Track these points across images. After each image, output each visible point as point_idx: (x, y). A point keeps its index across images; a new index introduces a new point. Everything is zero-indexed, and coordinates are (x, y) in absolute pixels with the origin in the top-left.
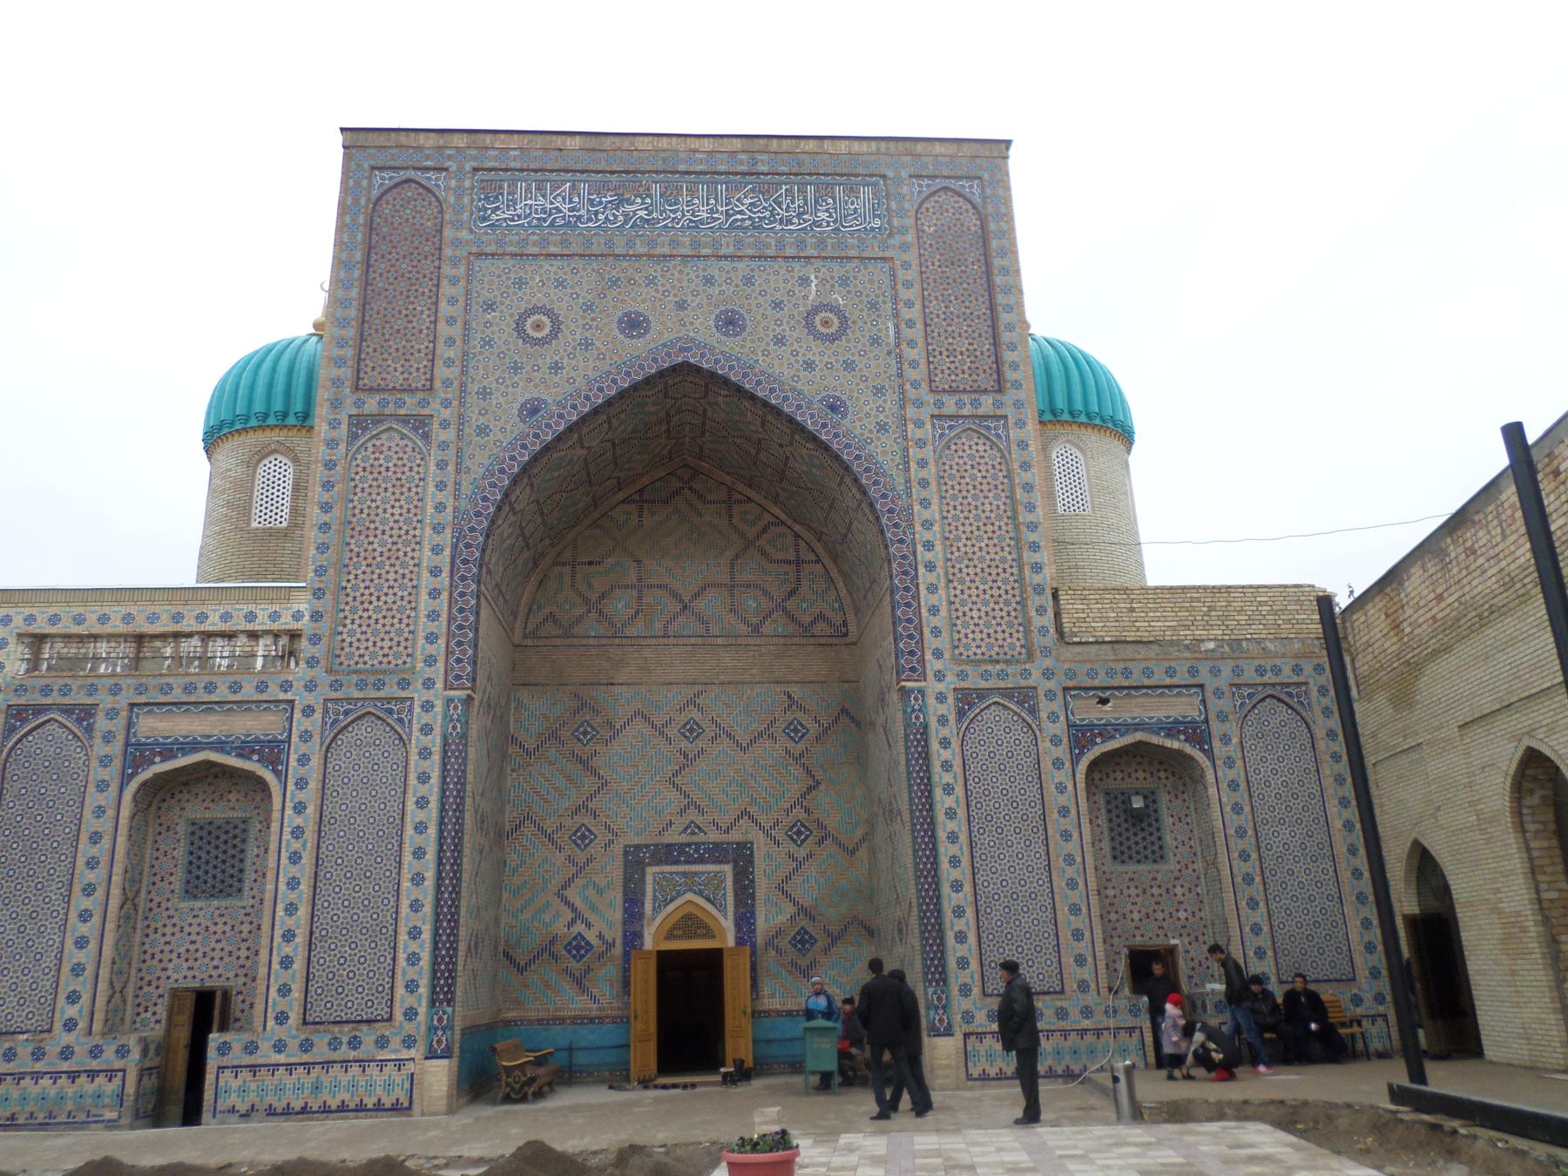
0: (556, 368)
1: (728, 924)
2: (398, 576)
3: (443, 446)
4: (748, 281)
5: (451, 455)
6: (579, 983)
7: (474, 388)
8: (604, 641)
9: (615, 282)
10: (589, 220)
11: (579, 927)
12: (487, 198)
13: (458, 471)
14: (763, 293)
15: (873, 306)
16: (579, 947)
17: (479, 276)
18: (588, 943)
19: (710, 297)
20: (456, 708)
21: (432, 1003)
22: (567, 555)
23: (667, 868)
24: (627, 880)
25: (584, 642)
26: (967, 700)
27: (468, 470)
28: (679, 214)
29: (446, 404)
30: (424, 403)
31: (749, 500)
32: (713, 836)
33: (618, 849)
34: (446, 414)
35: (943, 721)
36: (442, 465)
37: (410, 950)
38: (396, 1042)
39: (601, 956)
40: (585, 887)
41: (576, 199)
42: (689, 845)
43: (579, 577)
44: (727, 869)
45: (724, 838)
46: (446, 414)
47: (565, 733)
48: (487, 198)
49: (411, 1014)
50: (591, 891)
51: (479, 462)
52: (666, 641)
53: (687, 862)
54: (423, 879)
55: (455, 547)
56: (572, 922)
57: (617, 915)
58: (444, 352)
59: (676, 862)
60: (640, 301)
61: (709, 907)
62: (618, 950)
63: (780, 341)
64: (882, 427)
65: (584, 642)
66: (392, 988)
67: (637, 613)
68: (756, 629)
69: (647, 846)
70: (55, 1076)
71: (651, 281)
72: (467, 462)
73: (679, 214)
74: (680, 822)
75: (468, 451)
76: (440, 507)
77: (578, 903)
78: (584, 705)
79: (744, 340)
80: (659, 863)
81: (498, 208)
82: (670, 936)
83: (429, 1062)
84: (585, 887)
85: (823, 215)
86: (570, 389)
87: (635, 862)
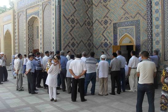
11: (106, 41)
16: (106, 45)
18: (108, 44)
24: (114, 30)
32: (131, 19)
33: (112, 24)
39: (110, 46)
44: (134, 27)
50: (108, 34)
56: (105, 40)
57: (113, 38)
59: (123, 26)
69: (118, 23)
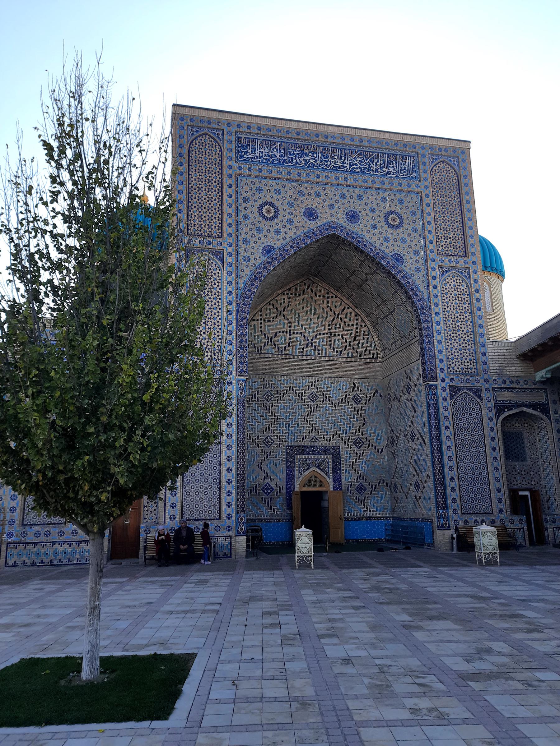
0: (277, 232)
1: (330, 481)
2: (213, 324)
3: (230, 265)
4: (360, 197)
5: (233, 269)
6: (268, 504)
7: (241, 238)
8: (275, 356)
9: (302, 194)
10: (289, 162)
11: (268, 481)
12: (242, 146)
13: (237, 277)
14: (366, 204)
15: (413, 214)
16: (268, 489)
17: (241, 184)
18: (271, 488)
19: (343, 204)
20: (242, 384)
21: (237, 512)
22: (258, 316)
23: (303, 456)
24: (287, 461)
25: (267, 356)
26: (454, 391)
27: (241, 277)
28: (329, 163)
29: (230, 245)
30: (220, 244)
31: (336, 296)
32: (323, 443)
33: (283, 447)
34: (230, 250)
35: (444, 399)
36: (229, 273)
37: (228, 489)
38: (223, 529)
39: (277, 493)
40: (270, 463)
41: (283, 151)
42: (314, 447)
43: (263, 326)
44: (330, 457)
45: (327, 444)
46: (230, 250)
47: (260, 396)
48: (242, 146)
49: (229, 517)
50: (272, 465)
51: (246, 272)
52: (301, 357)
53: (313, 454)
54: (231, 459)
55: (237, 312)
56: (264, 479)
57: (284, 476)
58: (227, 220)
59: (308, 454)
60: (313, 203)
61: (322, 473)
62: (284, 490)
63: (374, 227)
64: (418, 270)
65: (267, 356)
66: (220, 505)
67: (289, 344)
68: (340, 355)
69: (295, 446)
70: (70, 543)
71: (318, 194)
72: (240, 273)
73: (329, 163)
74: (309, 437)
75: (240, 268)
76: (230, 293)
77: (267, 471)
78: (267, 384)
79: (359, 225)
80: (301, 454)
81: (247, 152)
82: (306, 485)
83: (237, 537)
84: (270, 463)
85: (391, 169)
86: (284, 242)
87: (292, 452)
